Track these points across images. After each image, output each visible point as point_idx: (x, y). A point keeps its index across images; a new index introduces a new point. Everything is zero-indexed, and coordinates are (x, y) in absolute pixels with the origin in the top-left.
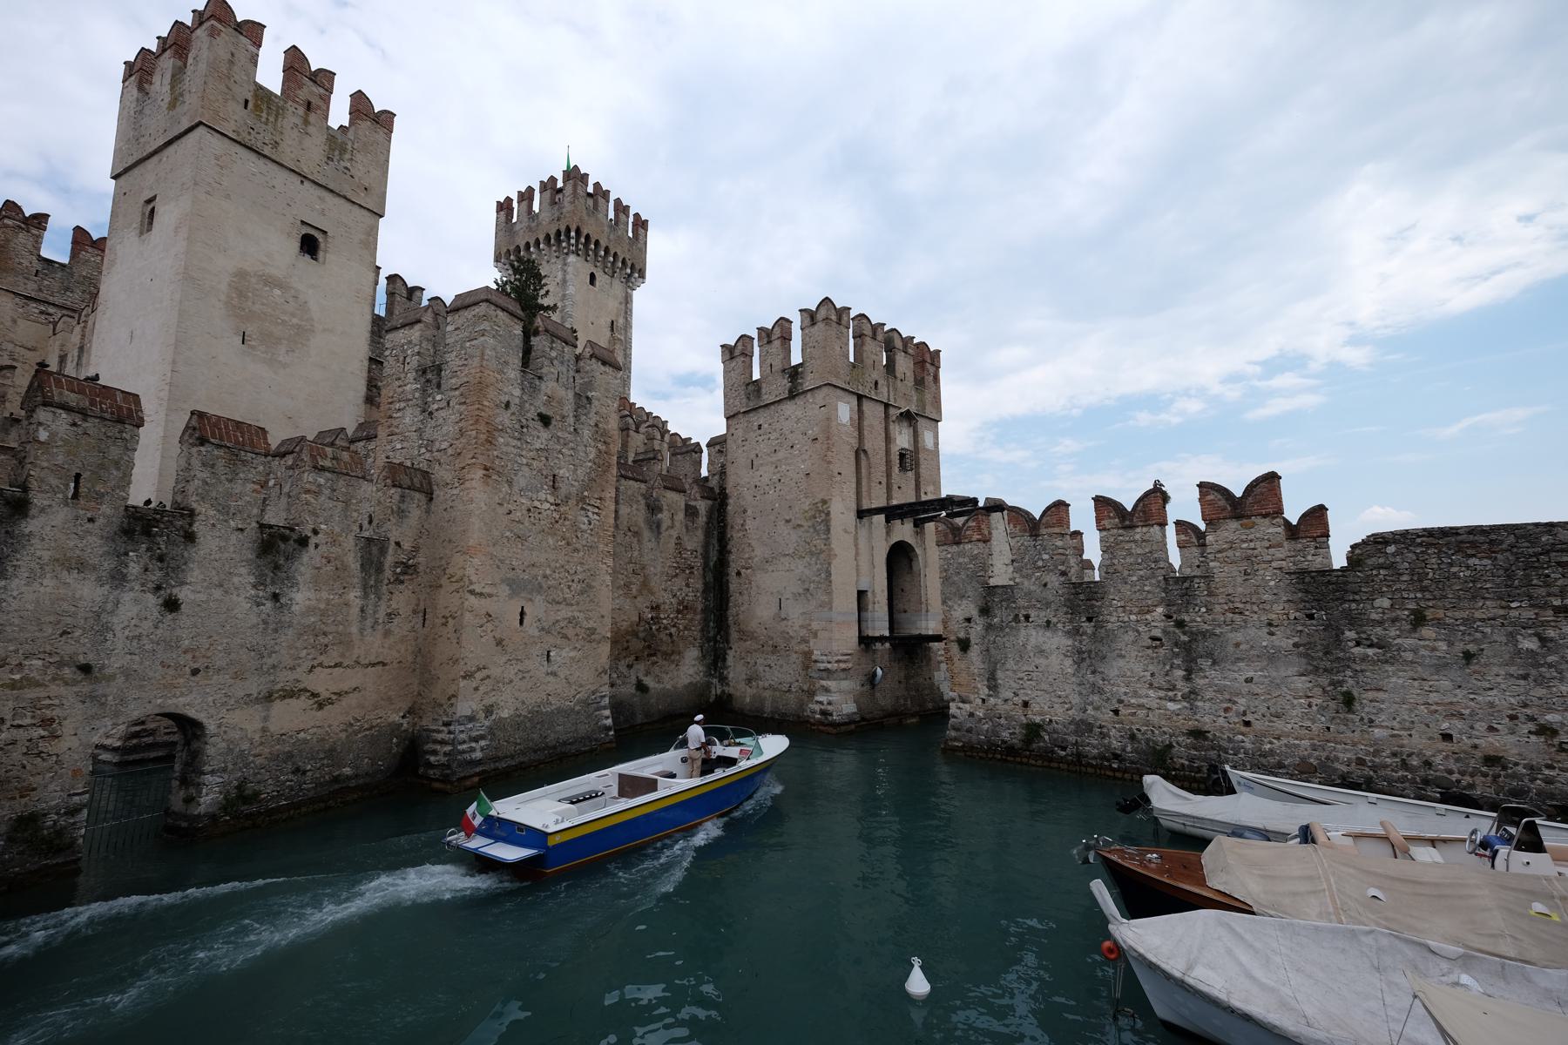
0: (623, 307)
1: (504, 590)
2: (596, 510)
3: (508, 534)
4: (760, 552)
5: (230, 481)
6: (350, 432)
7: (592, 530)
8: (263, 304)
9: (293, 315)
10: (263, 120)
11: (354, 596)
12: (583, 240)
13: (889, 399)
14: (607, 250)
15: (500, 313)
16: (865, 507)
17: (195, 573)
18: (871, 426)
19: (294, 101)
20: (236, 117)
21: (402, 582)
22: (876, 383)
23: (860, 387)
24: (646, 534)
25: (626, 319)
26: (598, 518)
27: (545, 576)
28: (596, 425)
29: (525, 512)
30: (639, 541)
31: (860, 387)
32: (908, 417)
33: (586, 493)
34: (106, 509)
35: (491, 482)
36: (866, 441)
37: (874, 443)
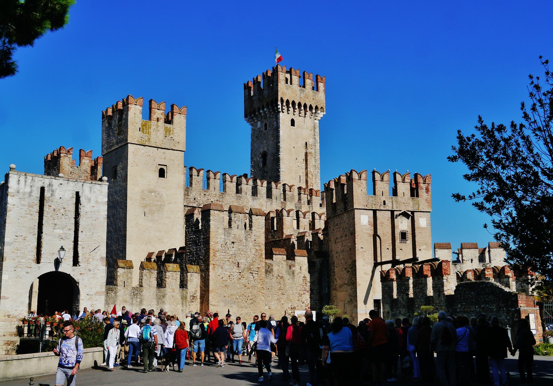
0: (312, 132)
1: (222, 304)
2: (257, 272)
3: (222, 285)
4: (338, 282)
5: (150, 278)
6: (178, 250)
7: (255, 280)
8: (149, 200)
9: (158, 201)
10: (145, 132)
11: (180, 307)
12: (285, 104)
13: (393, 208)
14: (300, 104)
15: (215, 211)
16: (379, 261)
17: (145, 302)
18: (382, 223)
19: (154, 120)
20: (137, 136)
21: (193, 302)
22: (384, 202)
23: (374, 206)
24: (286, 277)
25: (315, 139)
26: (257, 275)
27: (236, 298)
28: (255, 240)
29: (228, 277)
30: (283, 280)
31: (374, 206)
32: (405, 214)
33: (251, 267)
34: (129, 289)
35: (215, 269)
36: (378, 230)
37: (384, 230)
